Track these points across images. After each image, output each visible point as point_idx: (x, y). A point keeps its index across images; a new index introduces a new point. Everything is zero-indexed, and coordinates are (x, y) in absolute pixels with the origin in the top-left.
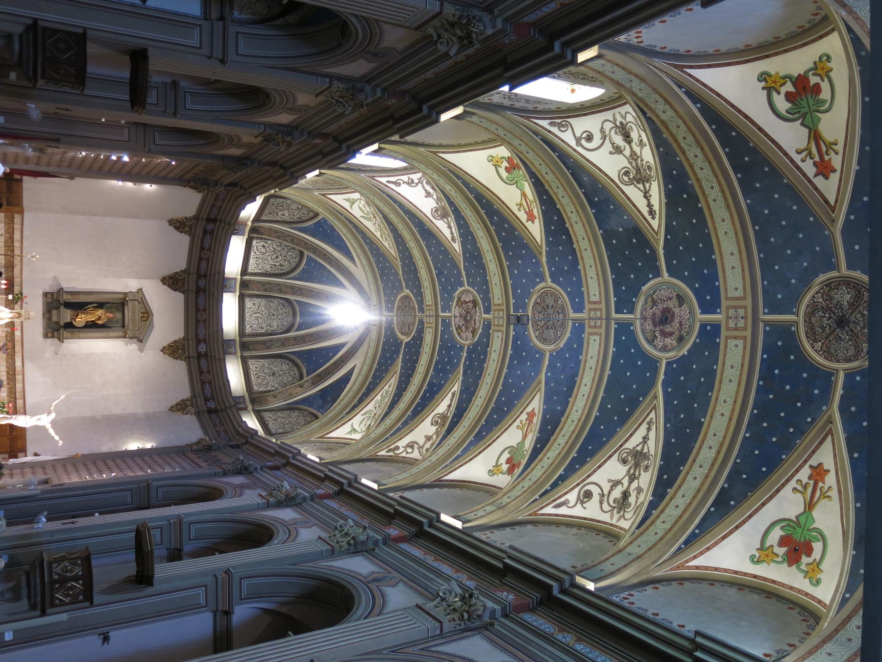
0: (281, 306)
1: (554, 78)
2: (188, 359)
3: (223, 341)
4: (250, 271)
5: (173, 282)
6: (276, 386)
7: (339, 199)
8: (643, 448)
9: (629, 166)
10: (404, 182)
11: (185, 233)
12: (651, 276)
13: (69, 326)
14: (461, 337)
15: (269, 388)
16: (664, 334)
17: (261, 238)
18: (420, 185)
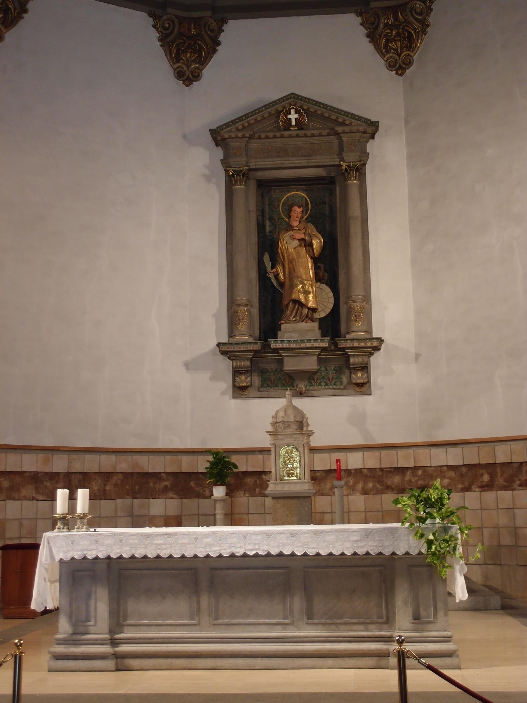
5: (189, 49)
13: (332, 325)
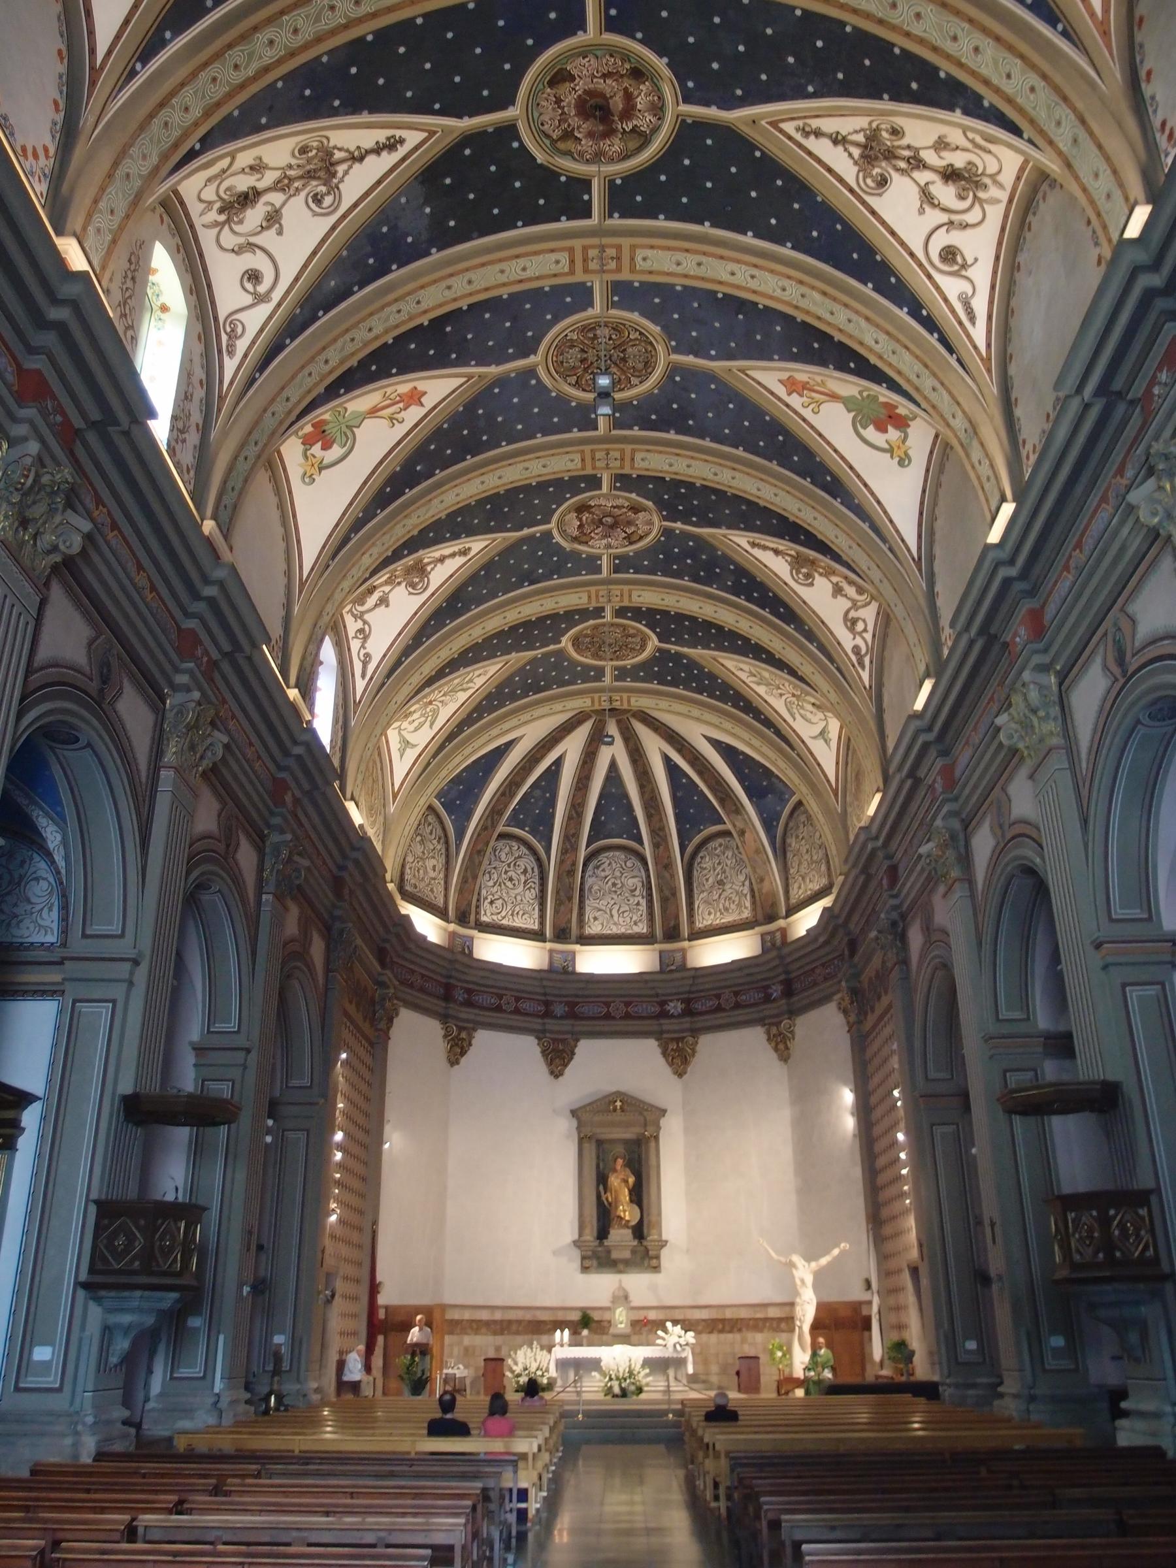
0: (598, 872)
1: (134, 339)
2: (696, 1032)
3: (662, 971)
4: (536, 927)
5: (558, 1057)
6: (742, 878)
8: (857, 144)
9: (303, 194)
10: (363, 646)
11: (471, 1037)
12: (515, 145)
13: (639, 1232)
14: (647, 535)
15: (746, 890)
16: (629, 112)
17: (478, 907)
18: (366, 617)
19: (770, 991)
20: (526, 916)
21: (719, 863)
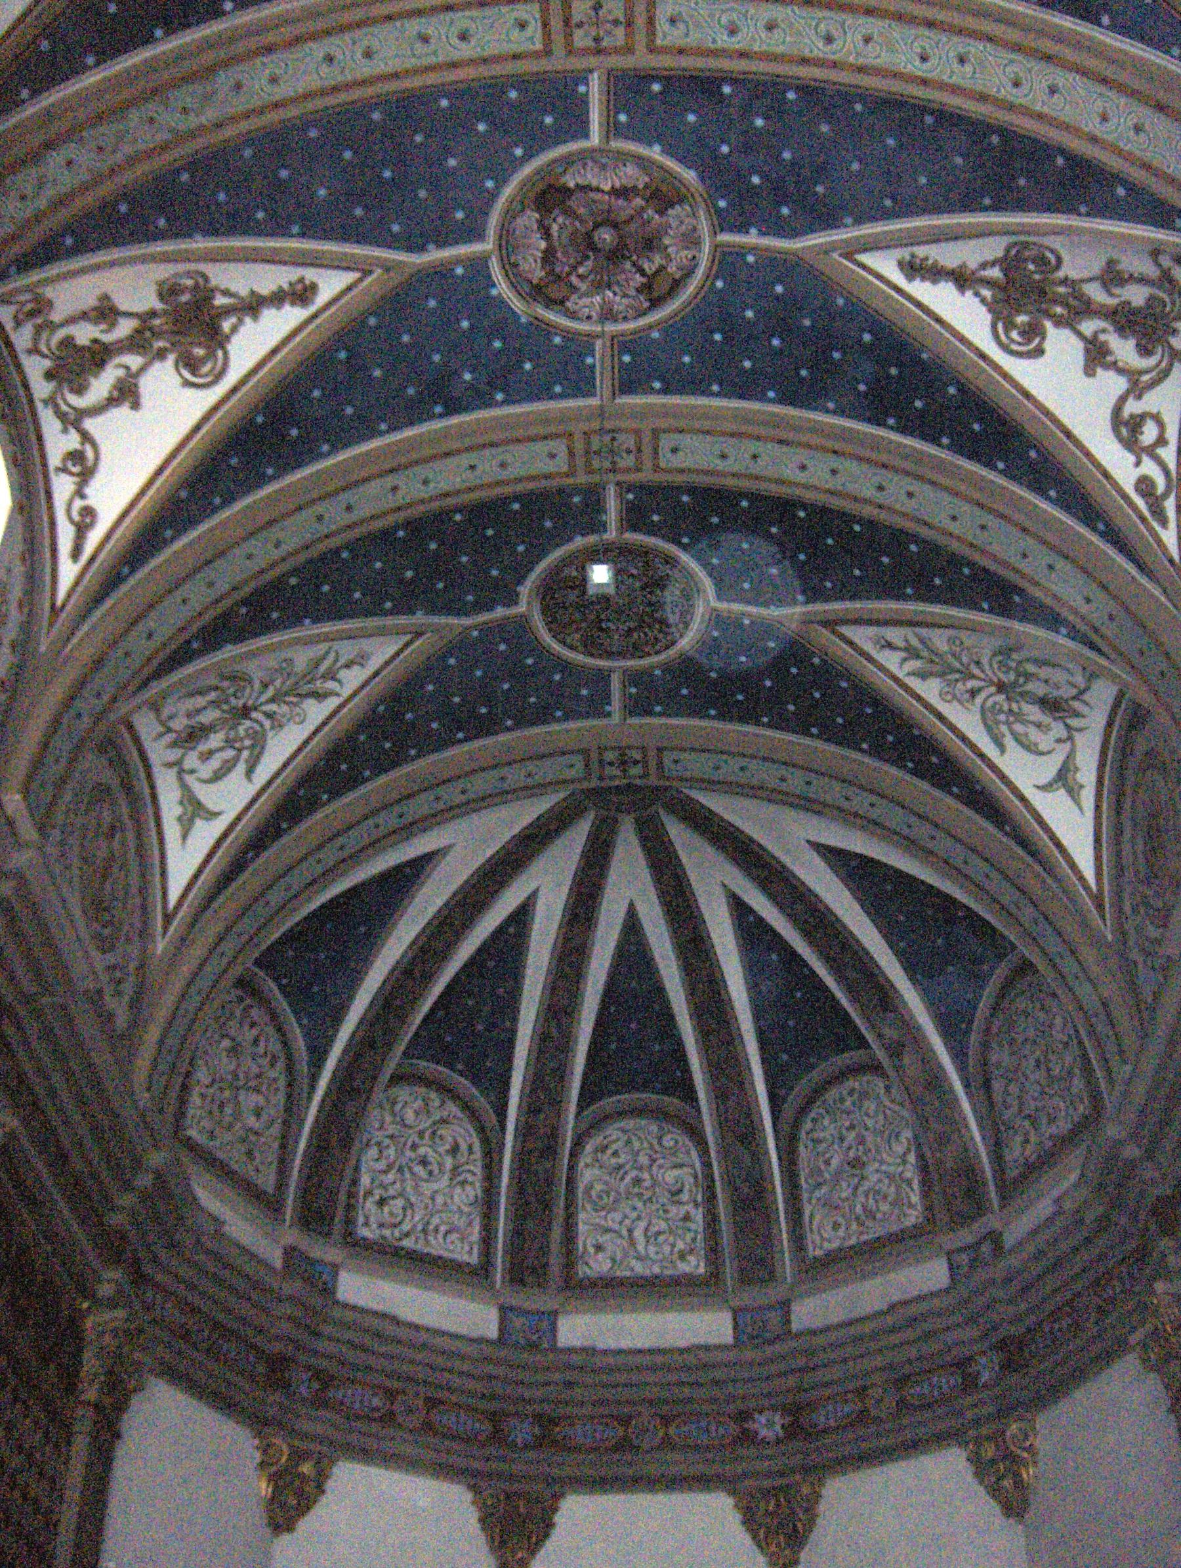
0: (606, 1157)
2: (819, 1470)
4: (474, 1259)
7: (185, 858)
10: (80, 493)
14: (689, 273)
17: (349, 1207)
18: (89, 424)
19: (974, 1368)
20: (454, 1236)
21: (852, 1127)
